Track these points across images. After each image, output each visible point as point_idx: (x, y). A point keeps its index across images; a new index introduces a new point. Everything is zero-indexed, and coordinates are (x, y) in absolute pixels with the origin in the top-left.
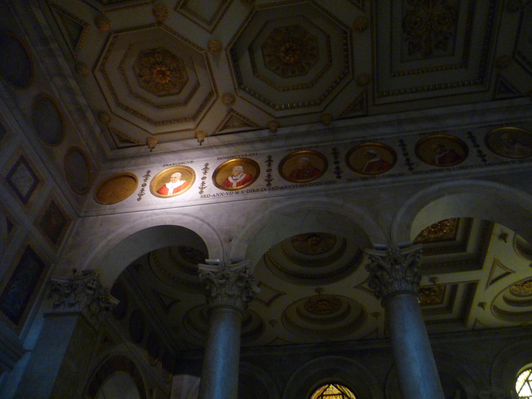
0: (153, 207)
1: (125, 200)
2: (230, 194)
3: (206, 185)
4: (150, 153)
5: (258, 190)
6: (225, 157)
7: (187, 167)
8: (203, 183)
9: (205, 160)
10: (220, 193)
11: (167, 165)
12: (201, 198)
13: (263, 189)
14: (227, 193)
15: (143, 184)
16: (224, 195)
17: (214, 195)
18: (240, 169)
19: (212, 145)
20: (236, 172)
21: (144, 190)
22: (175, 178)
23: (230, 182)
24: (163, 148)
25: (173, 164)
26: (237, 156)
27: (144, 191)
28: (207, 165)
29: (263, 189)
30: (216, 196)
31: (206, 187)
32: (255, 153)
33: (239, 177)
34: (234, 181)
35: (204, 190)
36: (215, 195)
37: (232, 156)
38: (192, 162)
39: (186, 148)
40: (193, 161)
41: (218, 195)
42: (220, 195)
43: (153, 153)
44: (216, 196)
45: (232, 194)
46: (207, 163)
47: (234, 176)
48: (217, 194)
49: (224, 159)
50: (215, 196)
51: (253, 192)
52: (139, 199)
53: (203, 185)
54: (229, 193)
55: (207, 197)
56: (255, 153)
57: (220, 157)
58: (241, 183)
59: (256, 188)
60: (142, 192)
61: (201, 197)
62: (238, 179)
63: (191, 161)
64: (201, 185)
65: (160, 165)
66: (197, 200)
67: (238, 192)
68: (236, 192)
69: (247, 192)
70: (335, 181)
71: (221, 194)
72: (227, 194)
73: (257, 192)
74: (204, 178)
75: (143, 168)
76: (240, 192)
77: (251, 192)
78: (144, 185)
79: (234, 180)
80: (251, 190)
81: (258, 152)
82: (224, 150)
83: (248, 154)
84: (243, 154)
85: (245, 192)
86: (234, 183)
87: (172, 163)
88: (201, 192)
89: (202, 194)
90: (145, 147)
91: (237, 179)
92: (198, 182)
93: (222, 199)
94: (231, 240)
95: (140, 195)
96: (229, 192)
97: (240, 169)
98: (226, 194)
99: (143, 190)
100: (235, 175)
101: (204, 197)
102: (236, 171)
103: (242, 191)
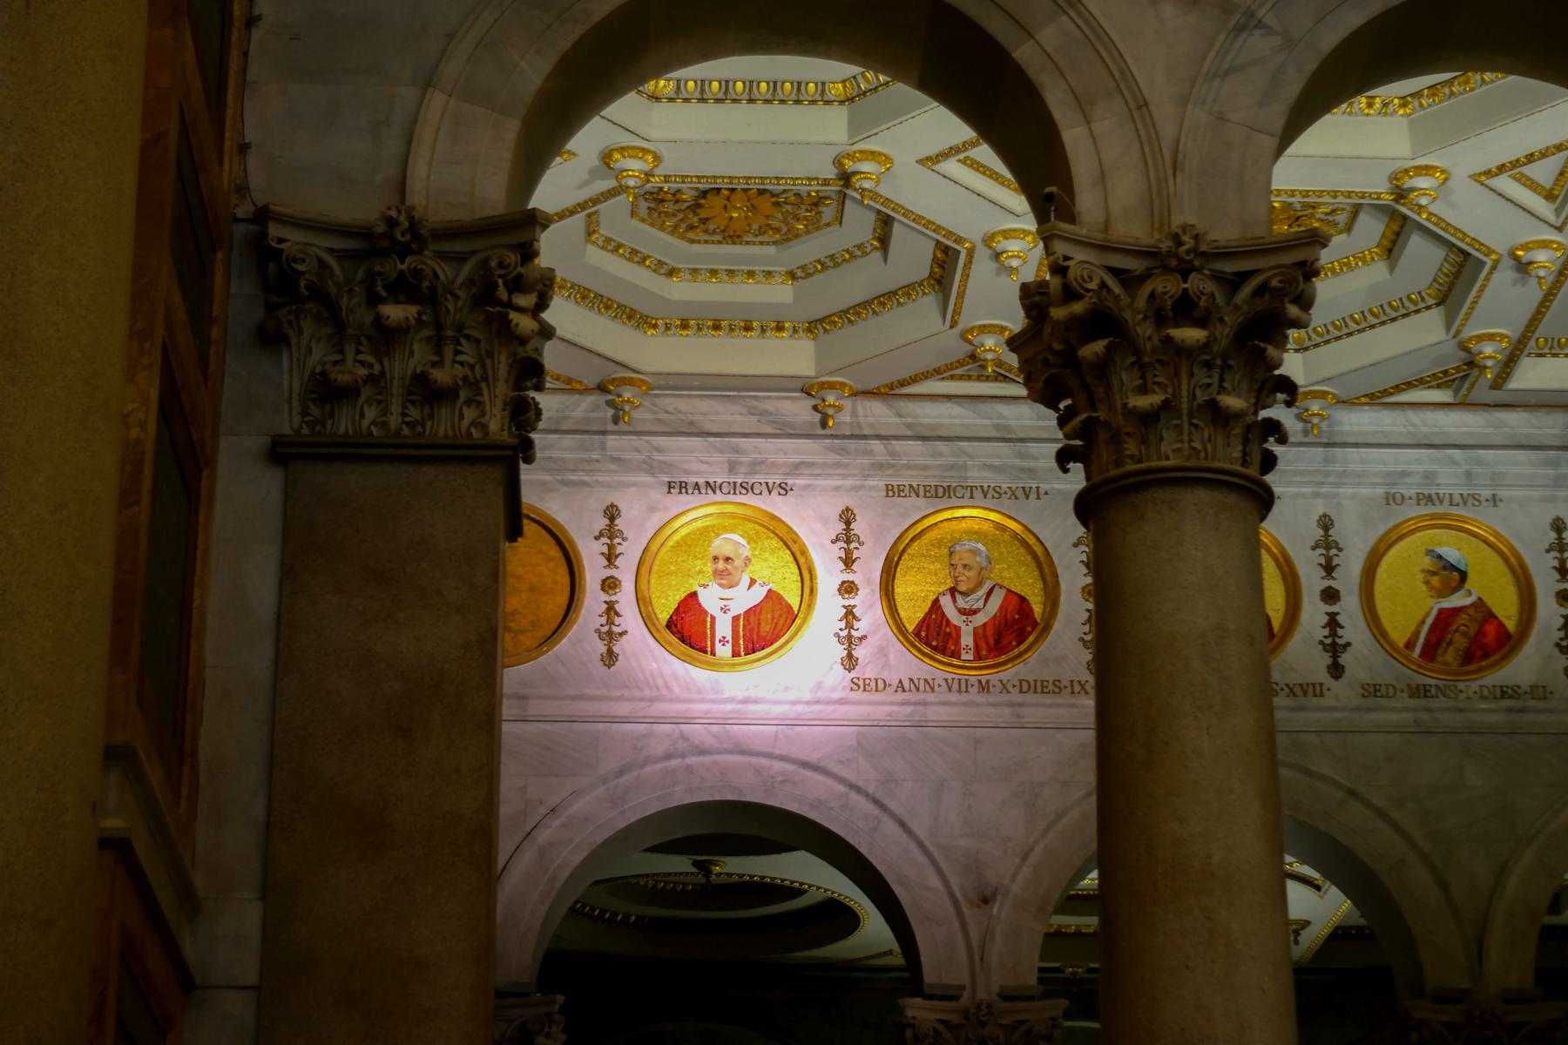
0: (676, 708)
1: (549, 653)
2: (960, 691)
3: (862, 627)
4: (611, 427)
5: (1057, 687)
6: (915, 484)
7: (773, 517)
8: (850, 615)
9: (837, 489)
10: (923, 676)
11: (683, 487)
12: (852, 689)
13: (1077, 688)
14: (946, 680)
15: (604, 581)
16: (936, 688)
17: (900, 682)
18: (978, 559)
19: (867, 431)
20: (967, 574)
21: (617, 614)
22: (727, 559)
23: (948, 621)
24: (668, 412)
25: (707, 483)
26: (963, 487)
27: (617, 620)
28: (847, 517)
29: (1077, 688)
30: (910, 690)
31: (864, 637)
32: (1034, 486)
33: (980, 604)
34: (964, 618)
35: (858, 652)
36: (906, 684)
37: (945, 485)
38: (784, 489)
39: (769, 430)
40: (790, 482)
41: (918, 689)
42: (922, 688)
43: (622, 426)
44: (910, 690)
45: (967, 691)
46: (848, 509)
47: (961, 593)
48: (911, 680)
49: (913, 494)
50: (904, 691)
51: (1042, 692)
52: (610, 658)
53: (849, 626)
54: (955, 686)
55: (877, 690)
56: (1034, 486)
57: (895, 484)
58: (990, 632)
59: (1048, 674)
60: (610, 622)
61: (855, 687)
62: (975, 612)
63: (778, 482)
64: (843, 625)
65: (648, 479)
66: (841, 701)
67: (988, 682)
68: (980, 681)
69: (1021, 692)
70: (1321, 685)
71: (926, 680)
72: (950, 689)
73: (1054, 693)
74: (848, 588)
75: (584, 484)
76: (994, 686)
77: (1035, 692)
78: (610, 585)
79: (962, 612)
80: (1035, 681)
81: (1044, 487)
82: (912, 450)
83: (1004, 486)
84: (986, 485)
85: (1014, 686)
86: (963, 627)
87: (701, 481)
88: (850, 662)
89: (853, 674)
90: (591, 399)
91: (975, 612)
92: (829, 605)
93: (936, 713)
94: (986, 901)
95: (610, 637)
96: (957, 677)
97: (978, 559)
98: (944, 684)
99: (611, 610)
100: (963, 588)
101: (865, 690)
102: (965, 566)
103: (1001, 681)
